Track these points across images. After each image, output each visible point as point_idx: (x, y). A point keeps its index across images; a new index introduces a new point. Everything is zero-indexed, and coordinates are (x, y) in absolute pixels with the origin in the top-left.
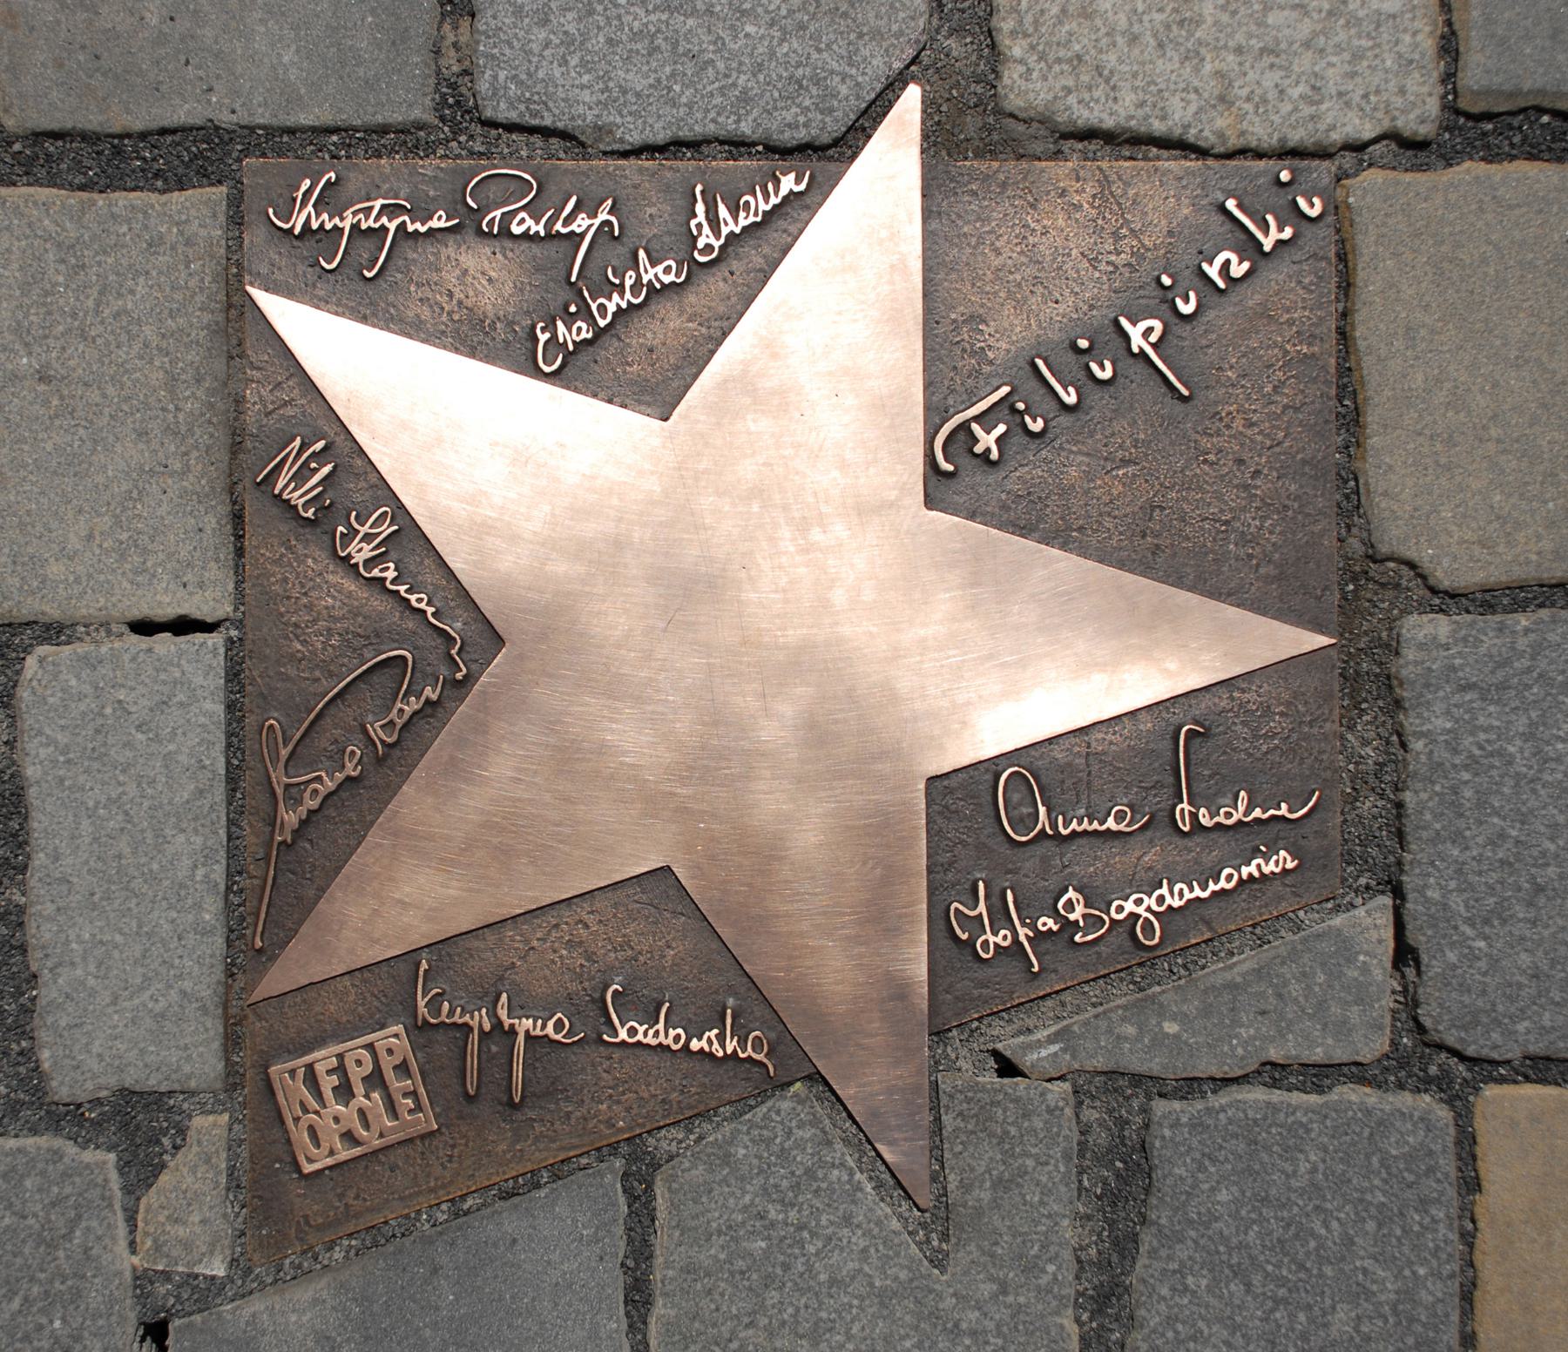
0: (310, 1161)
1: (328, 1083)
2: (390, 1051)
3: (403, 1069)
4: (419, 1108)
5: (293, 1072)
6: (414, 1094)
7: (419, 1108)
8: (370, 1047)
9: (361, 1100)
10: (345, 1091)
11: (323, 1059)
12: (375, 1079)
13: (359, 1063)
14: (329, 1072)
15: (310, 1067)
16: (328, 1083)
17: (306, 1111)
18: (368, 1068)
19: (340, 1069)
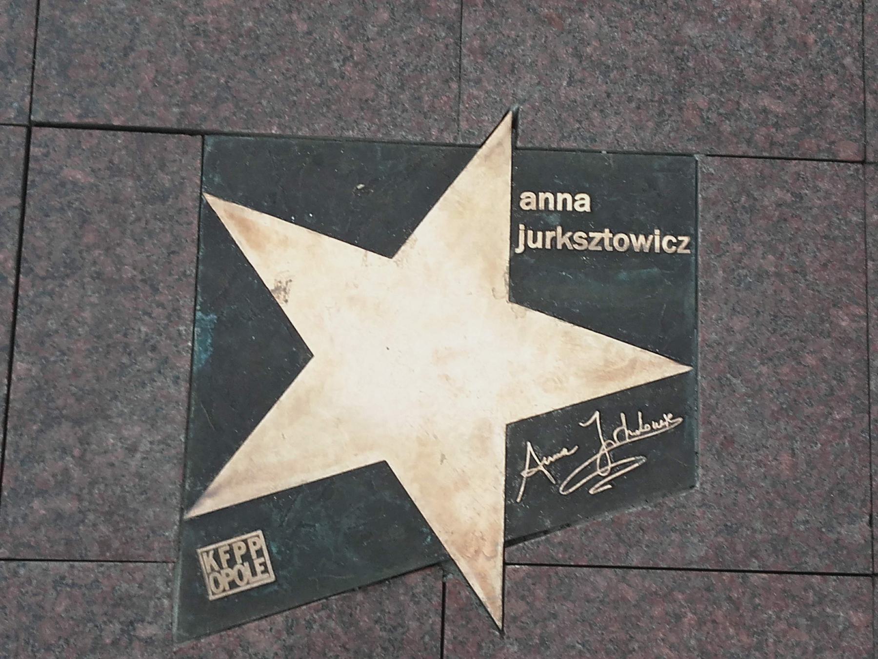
0: (213, 594)
1: (224, 558)
2: (254, 544)
3: (260, 553)
4: (266, 571)
5: (207, 552)
6: (264, 564)
7: (266, 571)
8: (245, 541)
9: (238, 566)
10: (231, 563)
11: (223, 545)
12: (247, 557)
13: (240, 548)
14: (226, 552)
15: (216, 551)
16: (224, 558)
17: (213, 569)
18: (243, 551)
19: (231, 552)
